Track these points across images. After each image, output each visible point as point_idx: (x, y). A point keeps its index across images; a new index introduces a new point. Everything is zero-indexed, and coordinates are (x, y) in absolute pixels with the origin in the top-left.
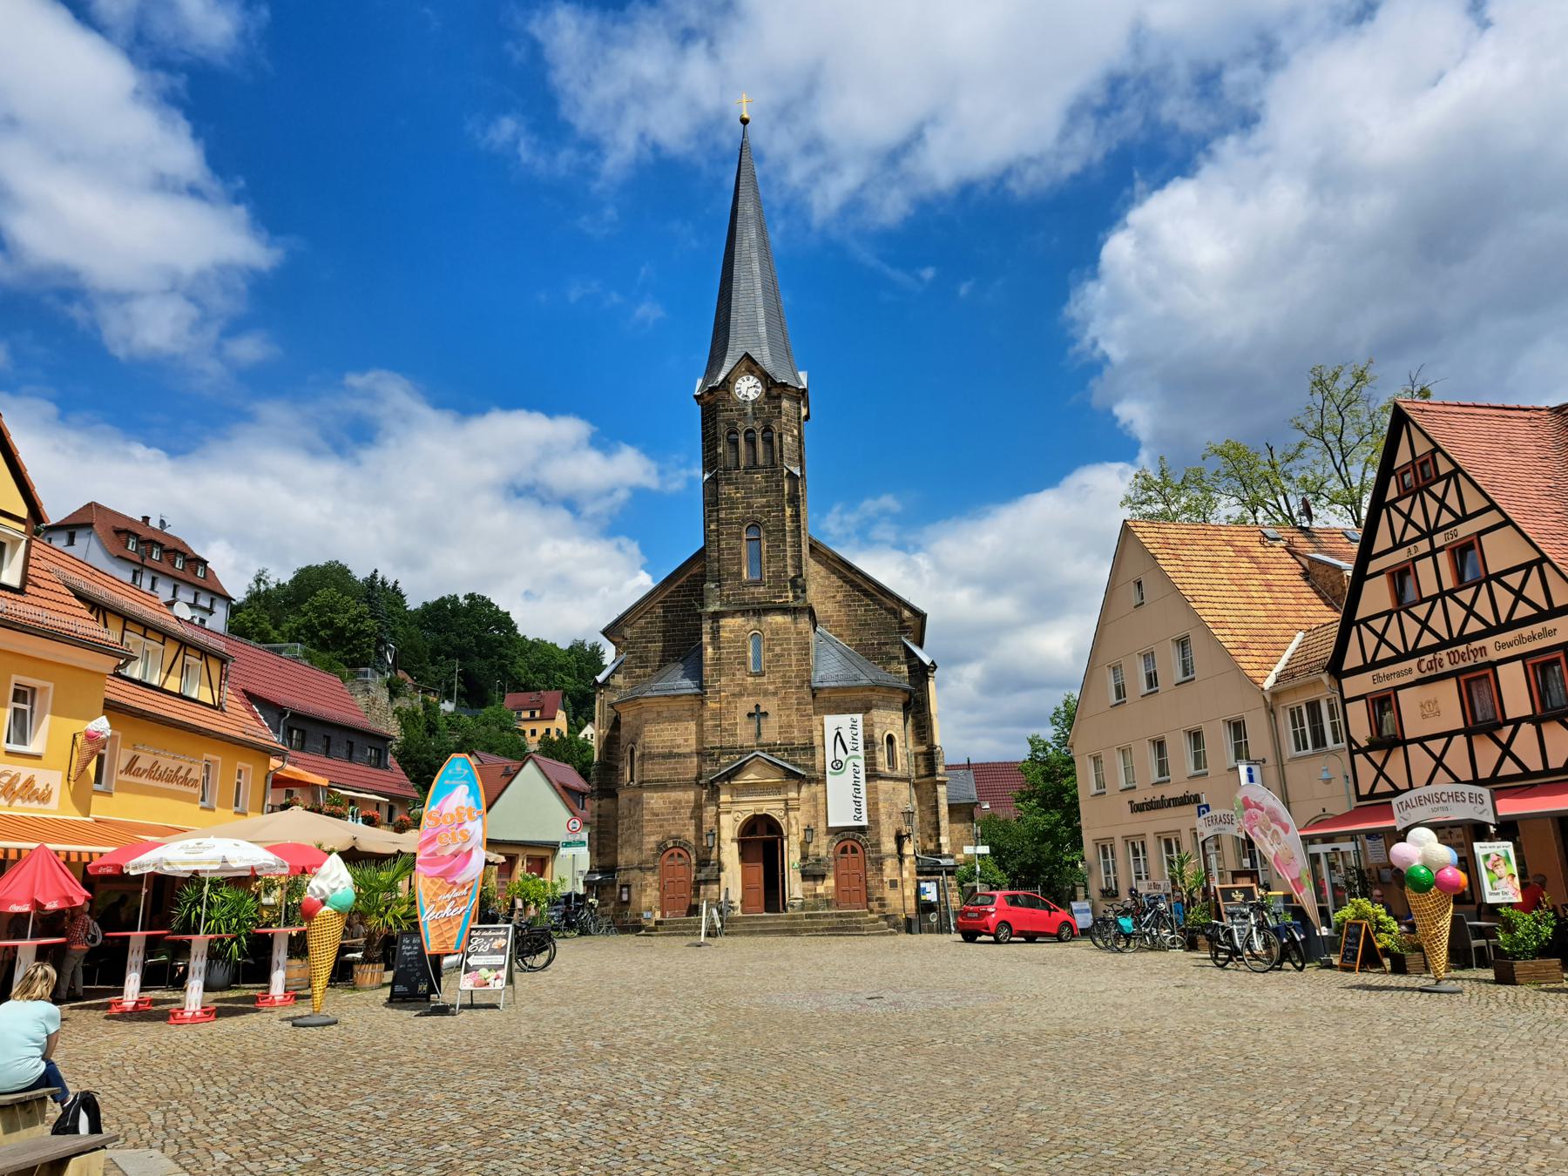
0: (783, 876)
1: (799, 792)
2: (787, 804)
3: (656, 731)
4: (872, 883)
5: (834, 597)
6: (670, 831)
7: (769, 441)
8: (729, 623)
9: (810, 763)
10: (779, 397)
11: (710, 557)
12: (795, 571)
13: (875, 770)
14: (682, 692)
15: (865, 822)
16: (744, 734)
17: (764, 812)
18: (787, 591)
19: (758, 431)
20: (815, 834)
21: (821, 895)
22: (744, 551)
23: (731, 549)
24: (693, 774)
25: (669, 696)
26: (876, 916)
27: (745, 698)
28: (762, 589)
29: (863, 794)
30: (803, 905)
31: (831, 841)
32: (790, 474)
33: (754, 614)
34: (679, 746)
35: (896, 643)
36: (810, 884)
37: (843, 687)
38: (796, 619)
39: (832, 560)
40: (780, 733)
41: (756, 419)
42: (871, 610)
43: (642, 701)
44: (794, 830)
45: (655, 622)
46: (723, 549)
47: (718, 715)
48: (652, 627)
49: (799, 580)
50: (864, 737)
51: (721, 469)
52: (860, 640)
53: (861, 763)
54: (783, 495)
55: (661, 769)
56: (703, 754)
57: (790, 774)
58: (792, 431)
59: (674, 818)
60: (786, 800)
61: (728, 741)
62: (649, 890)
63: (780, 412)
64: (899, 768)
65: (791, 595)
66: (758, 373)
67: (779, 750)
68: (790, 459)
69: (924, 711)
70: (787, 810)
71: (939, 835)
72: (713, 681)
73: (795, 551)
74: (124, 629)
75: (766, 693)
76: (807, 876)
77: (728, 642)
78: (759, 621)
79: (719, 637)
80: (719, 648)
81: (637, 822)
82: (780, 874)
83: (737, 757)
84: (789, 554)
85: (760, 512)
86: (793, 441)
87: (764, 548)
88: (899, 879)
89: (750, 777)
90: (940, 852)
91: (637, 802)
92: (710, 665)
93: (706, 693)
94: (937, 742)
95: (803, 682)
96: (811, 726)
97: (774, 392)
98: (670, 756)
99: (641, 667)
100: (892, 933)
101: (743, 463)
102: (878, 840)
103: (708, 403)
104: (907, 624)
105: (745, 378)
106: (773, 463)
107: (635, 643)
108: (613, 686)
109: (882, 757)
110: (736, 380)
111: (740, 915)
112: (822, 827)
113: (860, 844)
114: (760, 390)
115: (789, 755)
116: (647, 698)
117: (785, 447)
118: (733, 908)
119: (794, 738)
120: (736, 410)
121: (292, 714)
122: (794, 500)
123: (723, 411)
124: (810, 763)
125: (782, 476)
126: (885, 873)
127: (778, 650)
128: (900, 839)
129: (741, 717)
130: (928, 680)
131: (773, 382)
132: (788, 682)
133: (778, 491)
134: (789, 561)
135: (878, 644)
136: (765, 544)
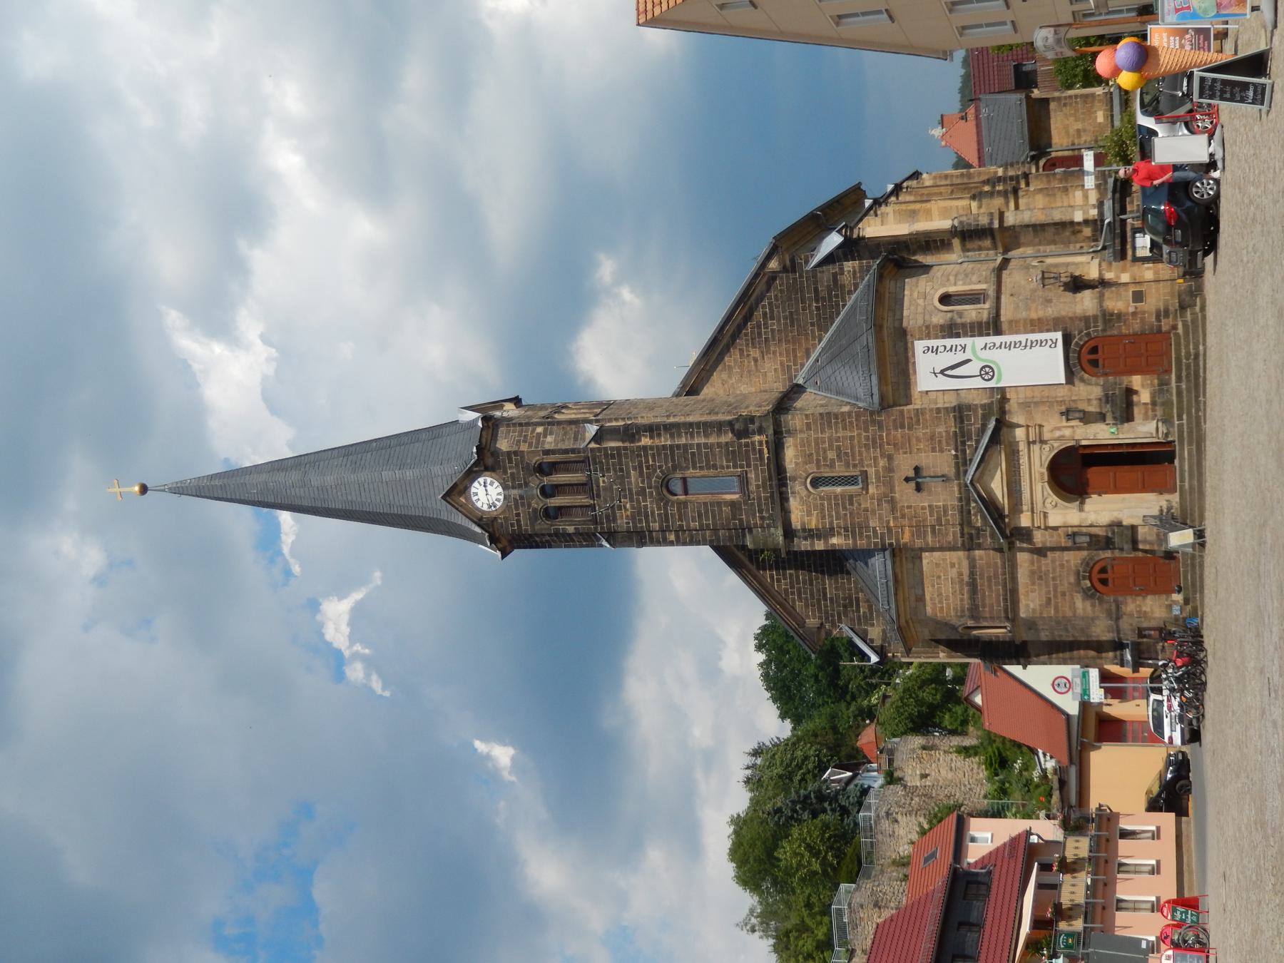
0: (1128, 445)
1: (1019, 426)
2: (1034, 442)
3: (941, 602)
4: (1136, 326)
5: (756, 360)
6: (1070, 584)
7: (553, 467)
8: (797, 518)
10: (496, 453)
12: (726, 433)
13: (988, 323)
14: (890, 572)
15: (1058, 336)
16: (944, 497)
17: (1045, 471)
18: (753, 443)
19: (542, 481)
20: (1073, 405)
21: (1153, 396)
22: (702, 498)
24: (997, 557)
25: (896, 590)
26: (1180, 326)
28: (752, 475)
29: (1022, 338)
30: (1167, 421)
31: (1082, 380)
32: (598, 438)
33: (786, 485)
34: (960, 574)
35: (815, 276)
36: (1137, 412)
37: (879, 368)
40: (941, 451)
41: (526, 484)
42: (771, 309)
43: (903, 621)
44: (1067, 432)
46: (701, 525)
47: (919, 529)
48: (805, 593)
49: (737, 427)
50: (943, 337)
51: (596, 529)
52: (813, 325)
53: (980, 341)
54: (625, 448)
55: (990, 596)
56: (970, 542)
57: (995, 439)
58: (539, 434)
59: (1054, 579)
60: (1029, 443)
61: (953, 516)
62: (1144, 609)
63: (516, 453)
64: (983, 286)
65: (757, 438)
66: (466, 482)
67: (964, 452)
68: (576, 439)
69: (905, 242)
70: (1043, 442)
71: (1072, 223)
72: (875, 536)
75: (890, 469)
76: (1126, 414)
77: (823, 517)
78: (794, 479)
79: (817, 529)
80: (832, 529)
84: (703, 440)
85: (649, 478)
86: (551, 433)
88: (1132, 289)
89: (997, 486)
90: (1095, 221)
91: (1031, 624)
93: (891, 545)
95: (873, 422)
96: (931, 410)
97: (489, 461)
98: (973, 586)
100: (1203, 309)
101: (583, 500)
102: (1080, 319)
103: (510, 542)
104: (788, 263)
105: (474, 498)
107: (827, 612)
109: (972, 313)
111: (1177, 494)
112: (1062, 393)
113: (1086, 342)
114: (489, 480)
118: (1169, 509)
120: (517, 508)
122: (630, 433)
126: (1124, 310)
127: (831, 455)
128: (1077, 284)
129: (921, 501)
130: (864, 238)
131: (475, 464)
133: (619, 455)
134: (713, 440)
135: (817, 301)
136: (690, 472)
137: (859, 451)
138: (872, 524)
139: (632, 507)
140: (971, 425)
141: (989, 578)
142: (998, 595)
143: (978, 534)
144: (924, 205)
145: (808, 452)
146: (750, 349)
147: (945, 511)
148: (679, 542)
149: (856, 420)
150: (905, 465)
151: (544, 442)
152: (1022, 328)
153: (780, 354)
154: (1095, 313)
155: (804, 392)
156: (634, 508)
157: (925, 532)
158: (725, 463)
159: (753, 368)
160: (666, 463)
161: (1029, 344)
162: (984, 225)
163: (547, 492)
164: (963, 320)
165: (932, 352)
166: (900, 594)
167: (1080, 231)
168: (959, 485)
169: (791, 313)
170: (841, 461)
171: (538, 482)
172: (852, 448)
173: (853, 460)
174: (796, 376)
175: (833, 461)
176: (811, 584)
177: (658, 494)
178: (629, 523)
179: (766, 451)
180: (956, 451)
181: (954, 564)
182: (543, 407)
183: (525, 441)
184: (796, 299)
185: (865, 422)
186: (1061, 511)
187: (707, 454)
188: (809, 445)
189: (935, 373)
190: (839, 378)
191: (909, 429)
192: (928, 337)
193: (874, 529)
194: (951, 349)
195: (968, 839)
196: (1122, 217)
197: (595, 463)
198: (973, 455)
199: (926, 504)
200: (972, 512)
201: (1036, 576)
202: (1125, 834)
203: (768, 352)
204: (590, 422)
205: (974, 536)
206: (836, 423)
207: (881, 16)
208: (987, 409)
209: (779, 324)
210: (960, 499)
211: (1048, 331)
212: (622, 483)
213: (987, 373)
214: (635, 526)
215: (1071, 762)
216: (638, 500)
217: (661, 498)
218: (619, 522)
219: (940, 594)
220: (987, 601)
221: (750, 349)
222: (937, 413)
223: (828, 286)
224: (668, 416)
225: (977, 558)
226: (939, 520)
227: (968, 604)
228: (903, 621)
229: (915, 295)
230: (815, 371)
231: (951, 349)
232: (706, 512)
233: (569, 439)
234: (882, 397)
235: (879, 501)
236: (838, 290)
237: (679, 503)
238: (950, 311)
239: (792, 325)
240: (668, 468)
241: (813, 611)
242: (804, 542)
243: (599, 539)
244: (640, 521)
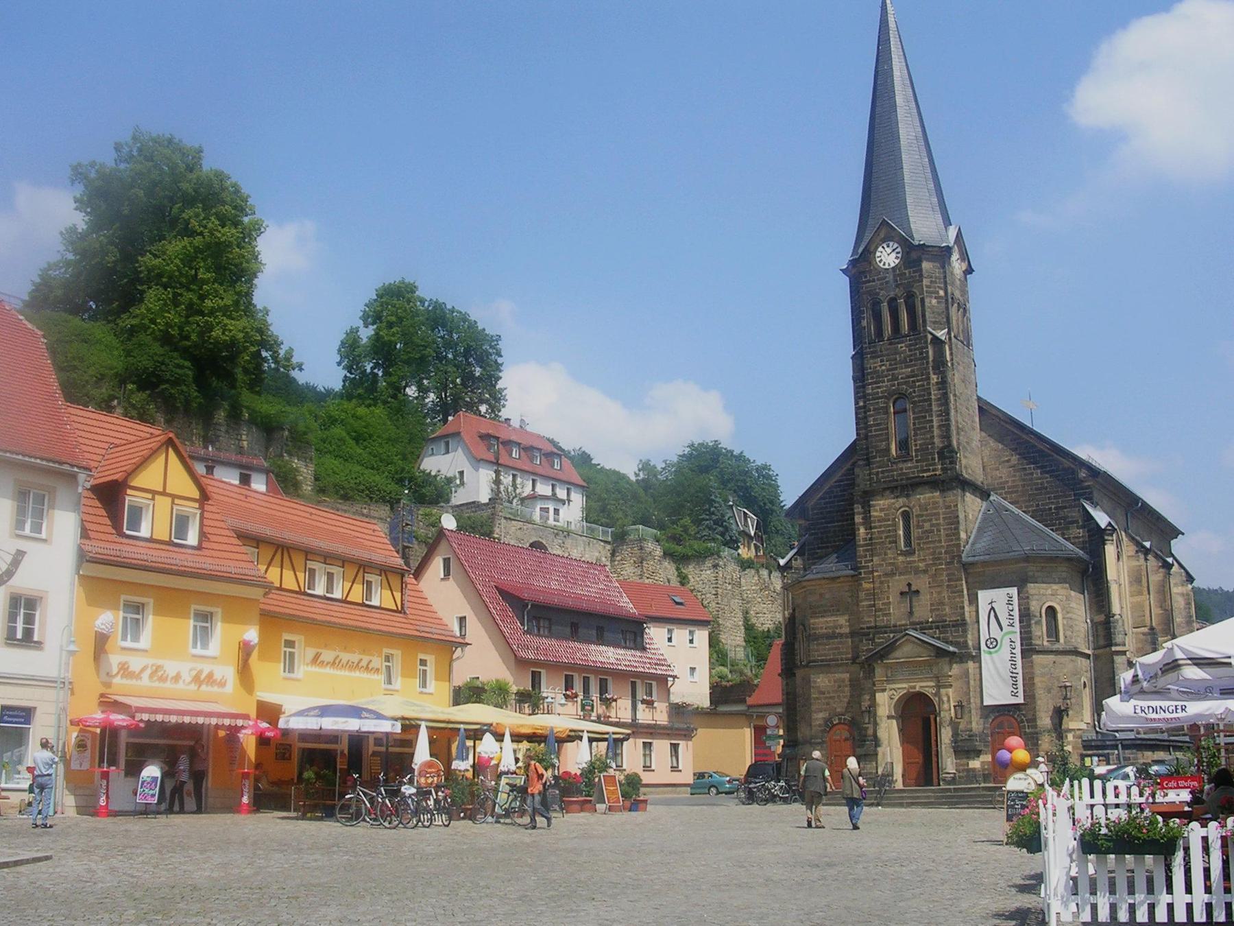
5: (1008, 461)
12: (943, 442)
13: (1031, 644)
16: (896, 612)
17: (917, 689)
18: (934, 464)
20: (966, 710)
27: (897, 577)
29: (1019, 670)
32: (936, 341)
34: (841, 627)
39: (1006, 423)
40: (931, 611)
41: (897, 286)
43: (804, 584)
44: (946, 706)
46: (871, 426)
52: (1038, 505)
54: (928, 363)
57: (941, 653)
61: (882, 621)
63: (921, 276)
64: (1062, 640)
65: (940, 467)
69: (1102, 577)
73: (942, 420)
74: (307, 559)
75: (917, 571)
79: (870, 516)
83: (892, 635)
84: (935, 424)
85: (905, 383)
86: (938, 302)
91: (807, 681)
92: (863, 546)
93: (860, 573)
95: (953, 558)
109: (1040, 632)
110: (877, 248)
115: (940, 633)
116: (808, 581)
119: (946, 615)
120: (878, 280)
121: (532, 605)
122: (940, 365)
124: (962, 640)
126: (1040, 748)
127: (927, 526)
129: (893, 598)
130: (1104, 544)
132: (939, 559)
134: (936, 432)
135: (1055, 508)
138: (875, 559)
139: (883, 371)
141: (839, 648)
144: (1146, 589)
148: (857, 409)
150: (921, 583)
151: (931, 297)
153: (1014, 481)
155: (982, 500)
157: (870, 600)
158: (919, 442)
159: (1002, 459)
161: (1014, 675)
162: (1115, 639)
163: (892, 303)
164: (1033, 626)
166: (823, 582)
171: (899, 295)
174: (996, 493)
175: (922, 527)
179: (929, 474)
180: (931, 622)
182: (964, 292)
183: (931, 282)
187: (925, 428)
190: (990, 528)
191: (948, 586)
194: (1010, 615)
195: (692, 629)
196: (1120, 746)
199: (891, 600)
202: (675, 747)
203: (1015, 471)
204: (949, 333)
206: (951, 529)
207: (375, 677)
210: (895, 626)
211: (1024, 691)
213: (991, 643)
214: (868, 374)
215: (750, 707)
217: (891, 394)
220: (821, 647)
224: (955, 395)
228: (804, 584)
230: (999, 509)
231: (1010, 615)
232: (881, 430)
233: (934, 317)
234: (972, 564)
235: (893, 564)
236: (1062, 525)
237: (887, 408)
238: (1041, 615)
239: (1036, 489)
241: (817, 514)
244: (872, 378)
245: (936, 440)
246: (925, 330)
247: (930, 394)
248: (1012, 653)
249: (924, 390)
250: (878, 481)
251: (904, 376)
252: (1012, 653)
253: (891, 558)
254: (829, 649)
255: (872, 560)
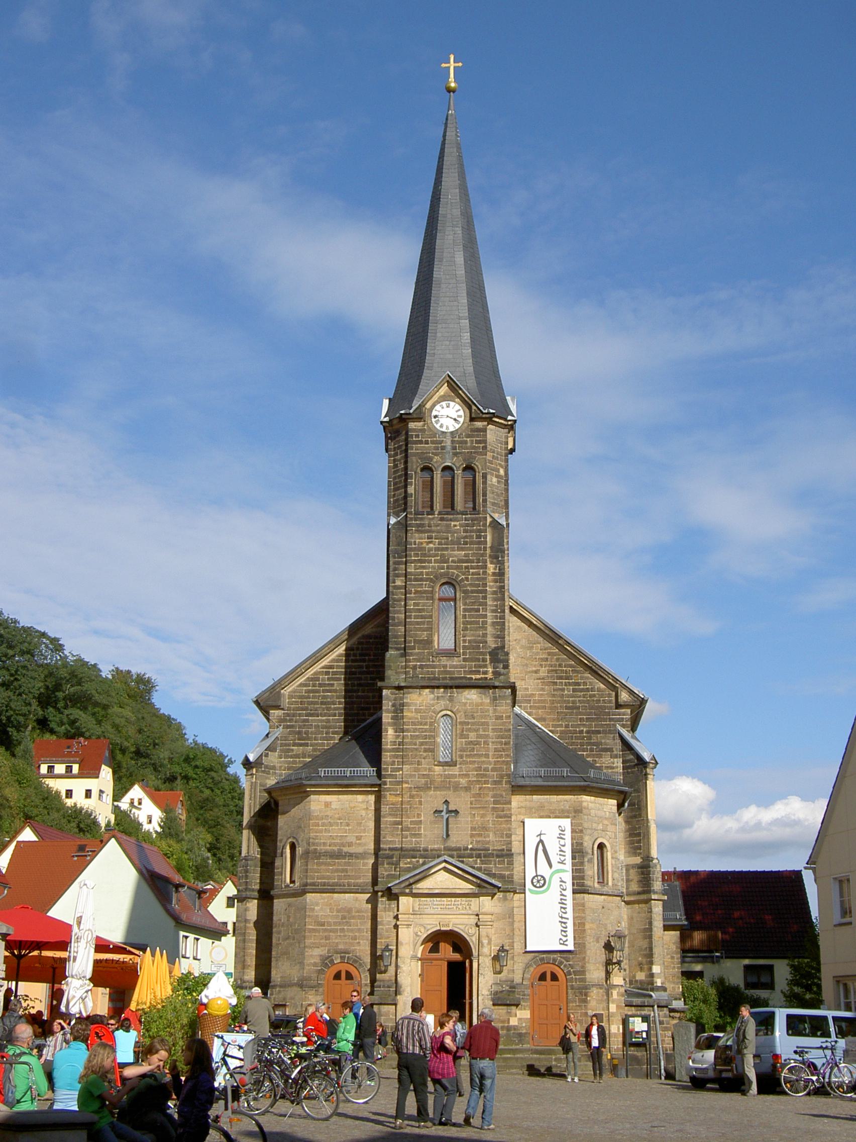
0: (471, 1004)
5: (536, 672)
9: (507, 873)
11: (394, 618)
13: (583, 885)
15: (571, 947)
18: (485, 666)
19: (458, 469)
21: (515, 1028)
23: (419, 611)
28: (456, 661)
29: (570, 914)
32: (495, 524)
34: (350, 844)
35: (610, 732)
38: (495, 699)
40: (472, 836)
41: (455, 454)
42: (581, 690)
44: (485, 950)
45: (318, 691)
48: (314, 697)
51: (411, 513)
52: (567, 726)
53: (568, 877)
54: (485, 549)
55: (328, 870)
58: (498, 471)
61: (410, 842)
63: (485, 448)
64: (610, 883)
65: (490, 670)
67: (471, 856)
68: (493, 504)
69: (640, 815)
71: (651, 963)
72: (393, 770)
73: (496, 617)
75: (456, 788)
77: (414, 724)
78: (451, 699)
80: (403, 731)
81: (297, 931)
82: (467, 1001)
83: (421, 861)
84: (489, 621)
85: (457, 568)
86: (499, 482)
87: (460, 613)
90: (652, 983)
92: (390, 751)
93: (385, 783)
94: (654, 853)
95: (502, 776)
96: (510, 829)
98: (339, 855)
99: (301, 745)
101: (438, 507)
102: (583, 967)
106: (474, 508)
108: (266, 767)
109: (591, 870)
112: (518, 947)
115: (482, 862)
117: (489, 488)
119: (488, 842)
120: (433, 442)
122: (499, 553)
123: (416, 442)
124: (507, 873)
125: (485, 525)
127: (472, 736)
129: (426, 816)
130: (646, 779)
132: (485, 776)
133: (479, 543)
134: (490, 630)
135: (588, 732)
137: (475, 761)
140: (495, 864)
141: (346, 871)
142: (329, 878)
143: (393, 864)
145: (475, 714)
146: (547, 668)
147: (415, 835)
149: (504, 761)
152: (577, 915)
154: (588, 980)
156: (429, 551)
160: (471, 585)
161: (564, 920)
164: (586, 863)
165: (560, 834)
167: (641, 970)
168: (440, 850)
169: (578, 708)
170: (466, 744)
172: (480, 756)
173: (466, 755)
175: (467, 737)
176: (322, 703)
177: (442, 575)
178: (415, 544)
179: (478, 676)
180: (472, 849)
181: (359, 840)
184: (590, 714)
185: (501, 769)
186: (412, 939)
187: (478, 623)
188: (482, 717)
189: (540, 835)
192: (573, 831)
193: (402, 769)
194: (561, 851)
197: (473, 520)
198: (467, 864)
199: (422, 818)
200: (413, 860)
201: (346, 914)
205: (390, 860)
206: (501, 743)
208: (508, 880)
209: (568, 696)
210: (426, 850)
212: (453, 543)
213: (538, 881)
214: (411, 550)
216: (436, 555)
218: (417, 535)
219: (331, 825)
220: (323, 867)
221: (547, 668)
222: (506, 834)
223: (601, 743)
225: (366, 861)
226: (408, 829)
227: (321, 850)
229: (606, 822)
231: (561, 851)
232: (422, 617)
233: (494, 499)
238: (593, 852)
239: (567, 708)
240: (465, 586)
242: (390, 704)
243: (397, 515)
244: (416, 555)
245: (490, 639)
246: (485, 512)
247: (485, 585)
248: (562, 895)
249: (478, 579)
250: (415, 676)
251: (456, 559)
252: (562, 895)
253: (425, 769)
254: (334, 871)
255: (402, 769)
